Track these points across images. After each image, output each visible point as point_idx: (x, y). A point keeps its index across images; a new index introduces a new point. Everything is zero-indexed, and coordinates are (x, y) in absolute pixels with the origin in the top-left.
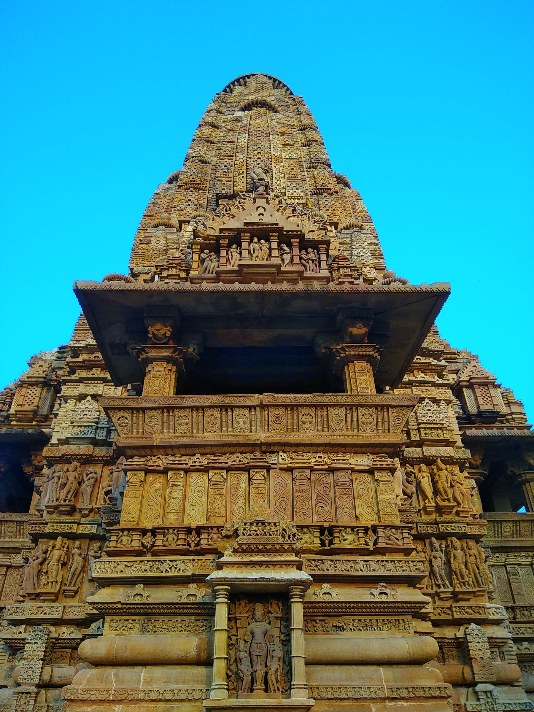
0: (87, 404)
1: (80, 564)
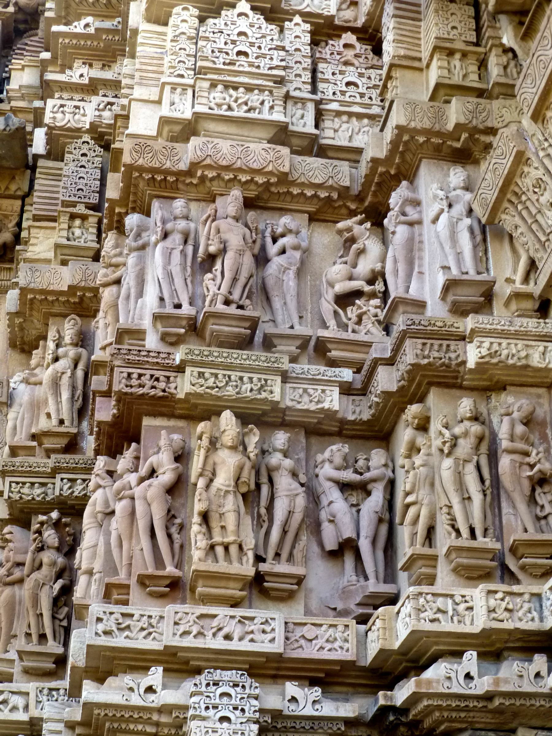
0: (243, 25)
1: (301, 501)
